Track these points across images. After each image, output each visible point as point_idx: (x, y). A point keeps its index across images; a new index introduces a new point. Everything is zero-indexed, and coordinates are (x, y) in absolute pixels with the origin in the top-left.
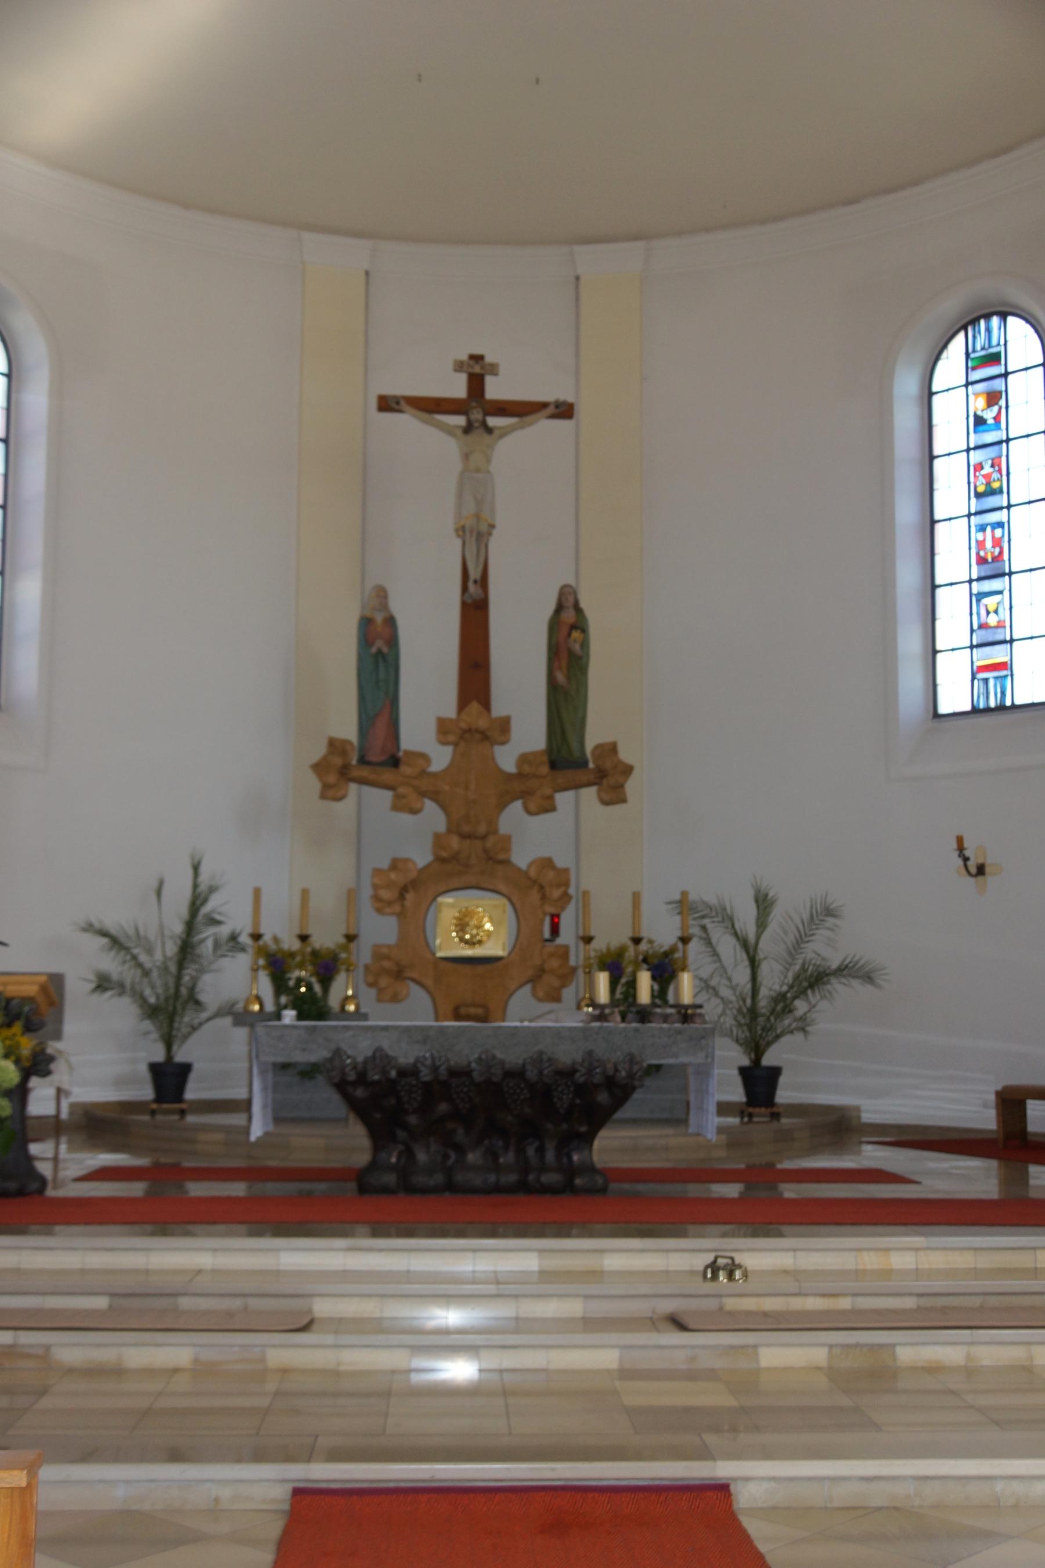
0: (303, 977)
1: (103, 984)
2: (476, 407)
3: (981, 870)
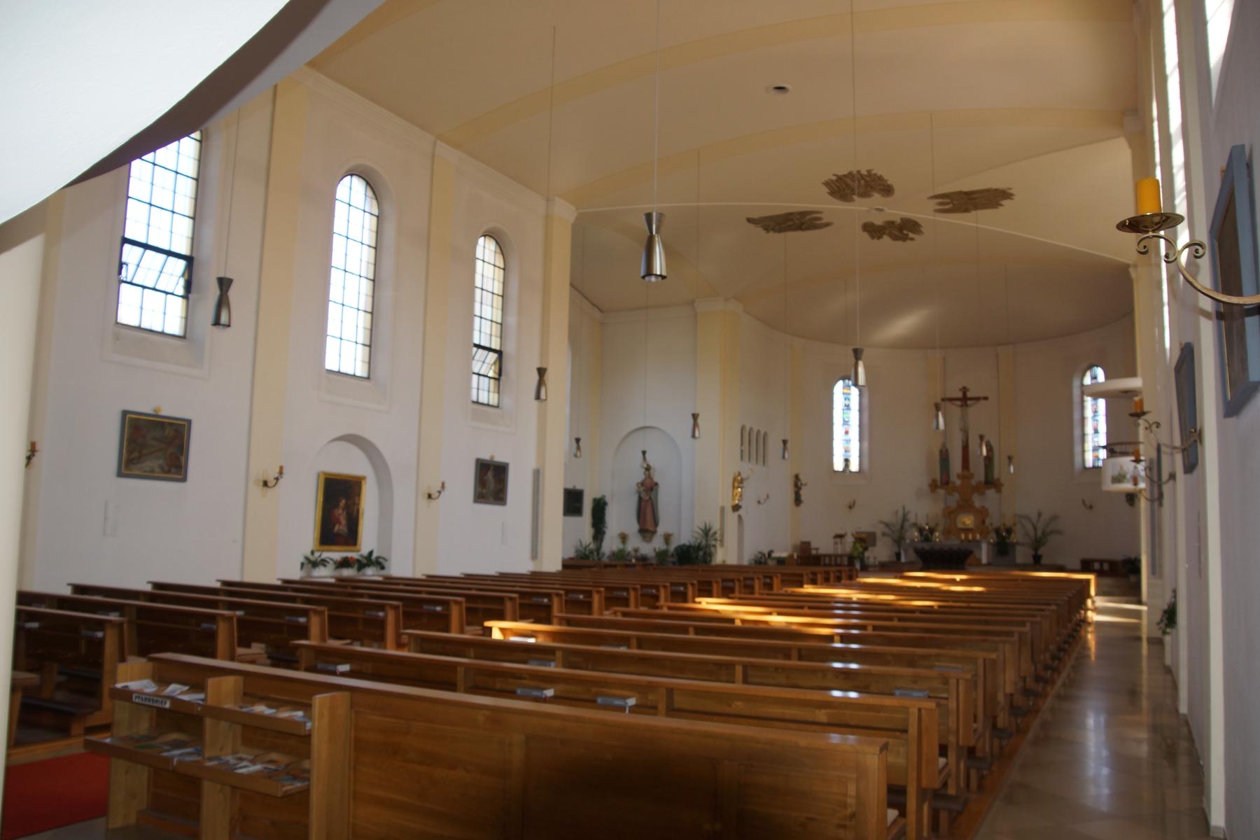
0: (926, 535)
1: (884, 534)
2: (965, 400)
3: (1091, 507)
